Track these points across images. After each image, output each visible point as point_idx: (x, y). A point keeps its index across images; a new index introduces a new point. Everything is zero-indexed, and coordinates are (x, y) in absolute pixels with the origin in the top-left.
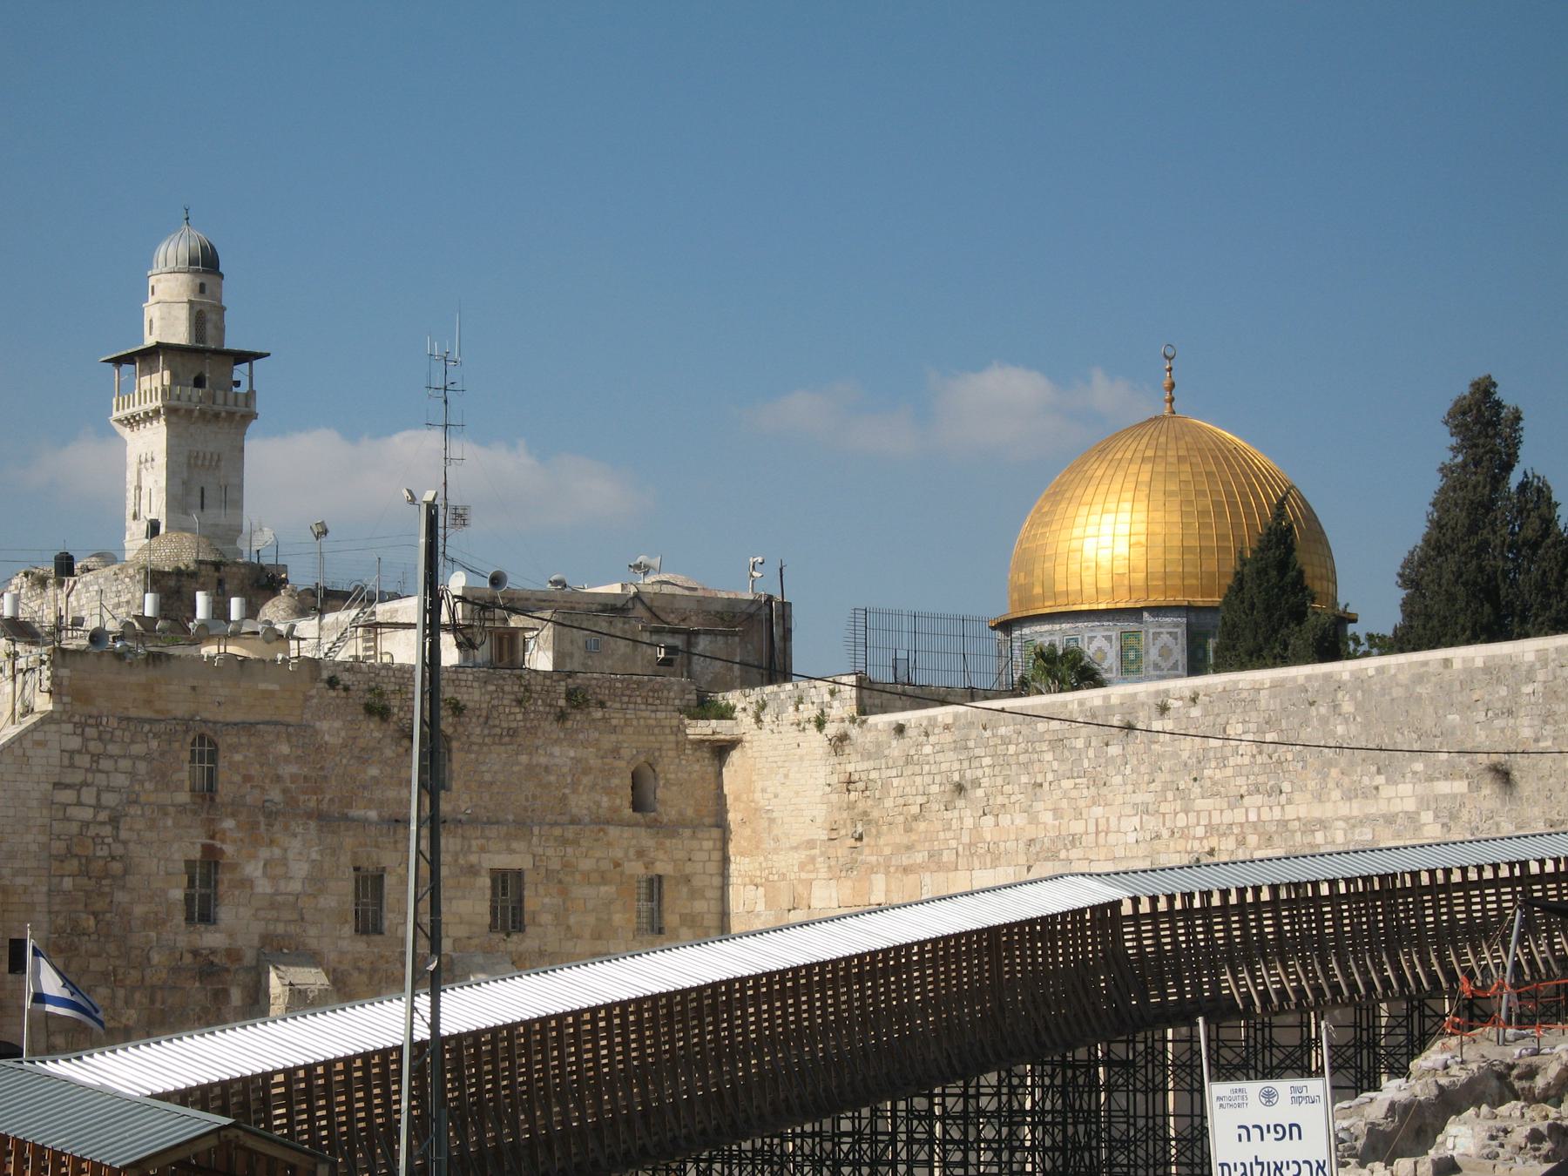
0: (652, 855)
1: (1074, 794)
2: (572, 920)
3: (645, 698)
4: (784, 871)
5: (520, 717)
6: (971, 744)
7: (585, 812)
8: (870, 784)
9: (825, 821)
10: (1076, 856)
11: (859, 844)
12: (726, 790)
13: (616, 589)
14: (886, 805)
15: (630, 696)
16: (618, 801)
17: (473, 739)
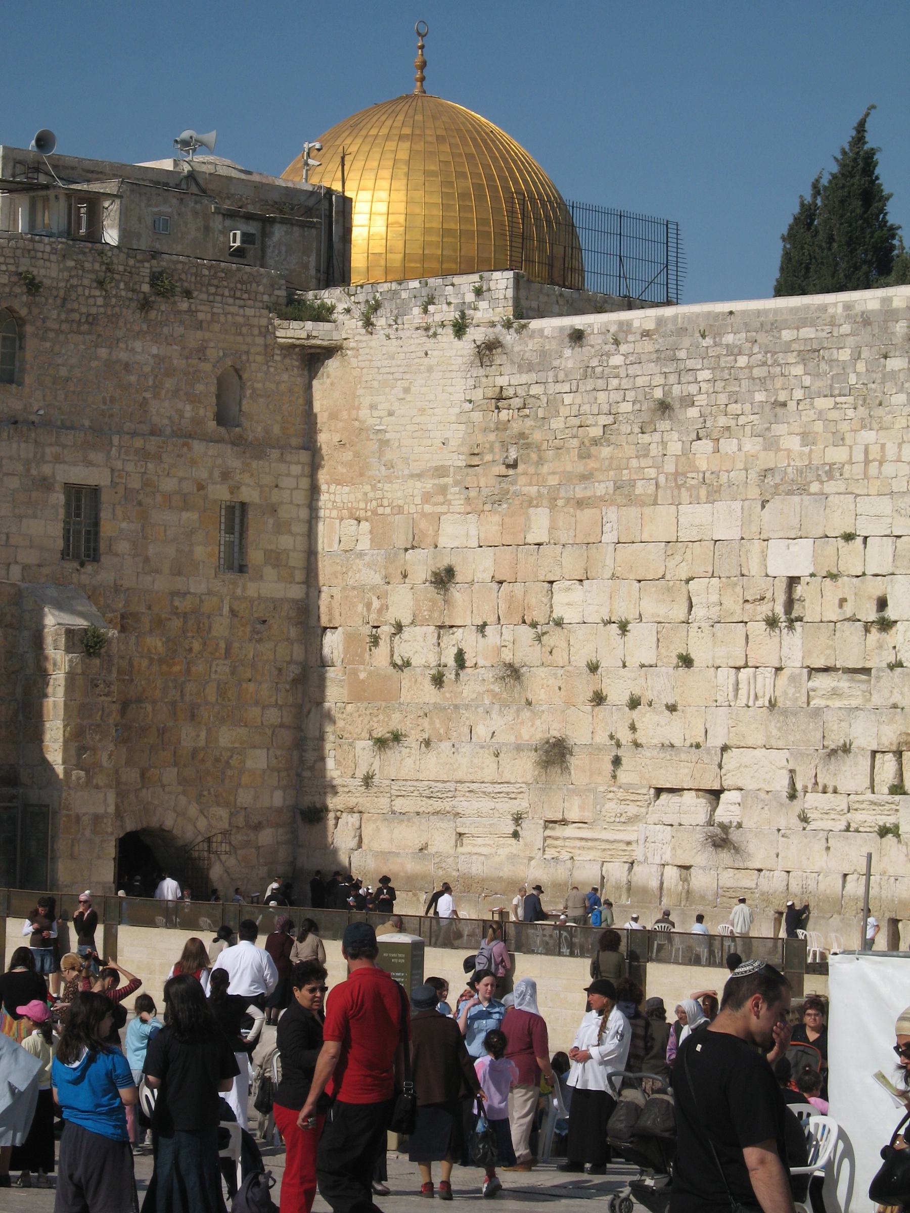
0: (238, 477)
1: (834, 415)
2: (151, 550)
3: (233, 290)
4: (401, 502)
5: (100, 301)
6: (682, 354)
7: (166, 422)
8: (530, 401)
9: (462, 444)
10: (834, 490)
11: (511, 472)
12: (317, 407)
13: (167, 164)
14: (553, 426)
15: (217, 287)
16: (202, 412)
17: (49, 324)
